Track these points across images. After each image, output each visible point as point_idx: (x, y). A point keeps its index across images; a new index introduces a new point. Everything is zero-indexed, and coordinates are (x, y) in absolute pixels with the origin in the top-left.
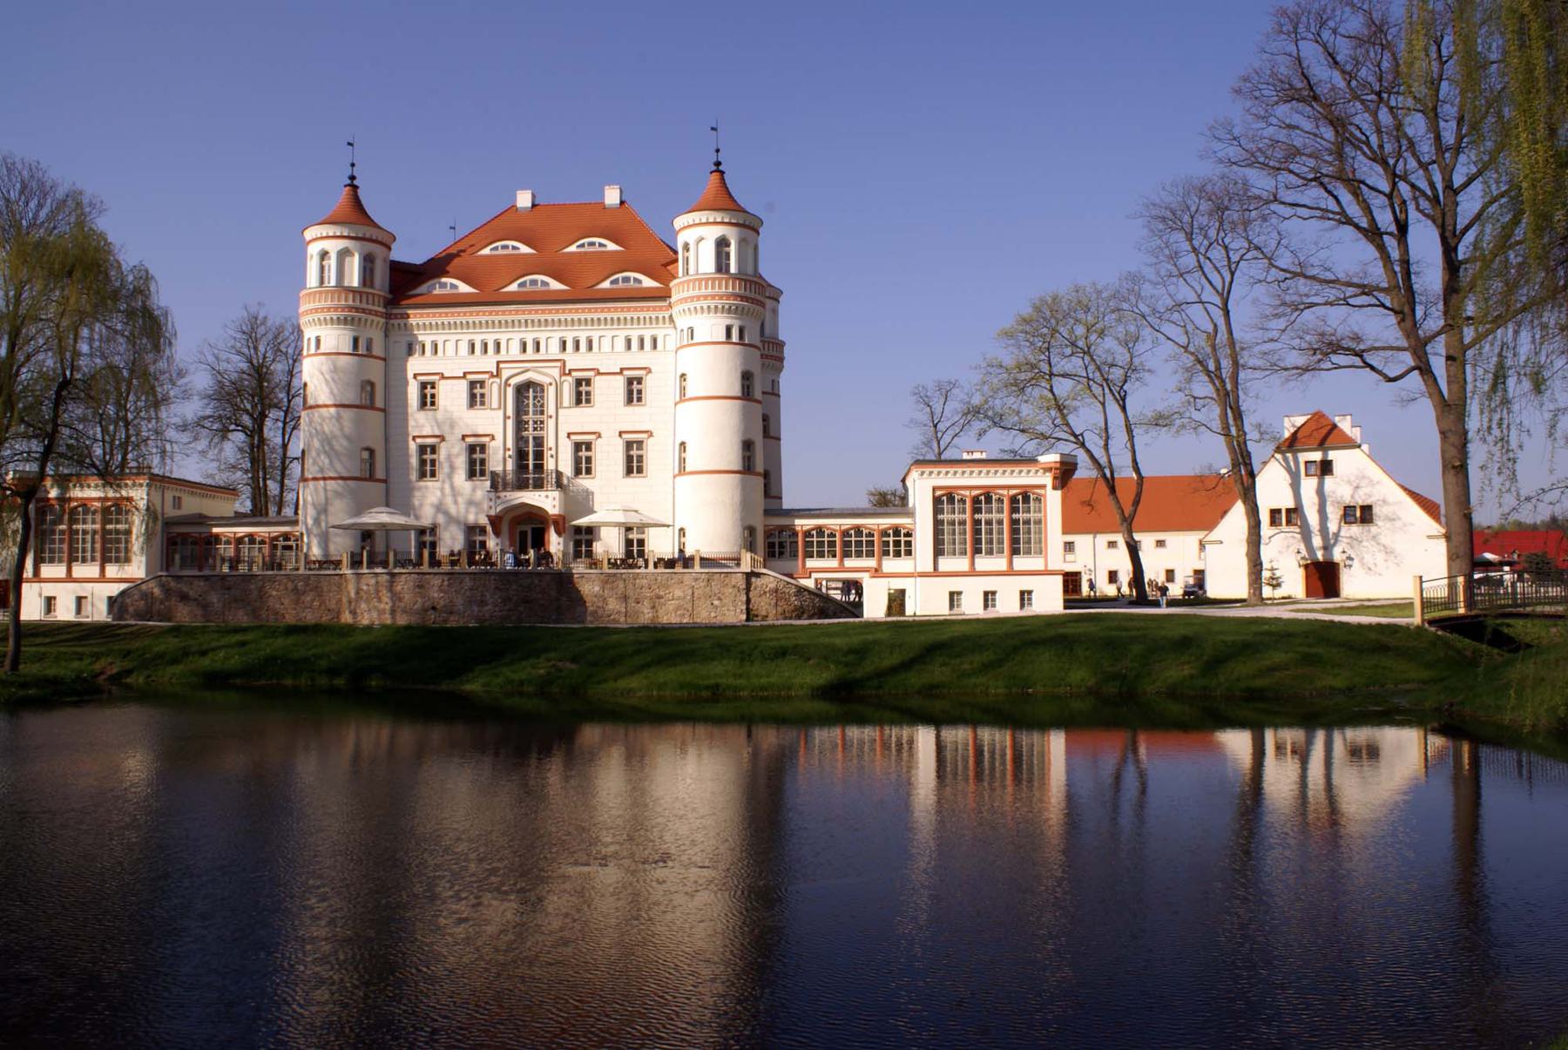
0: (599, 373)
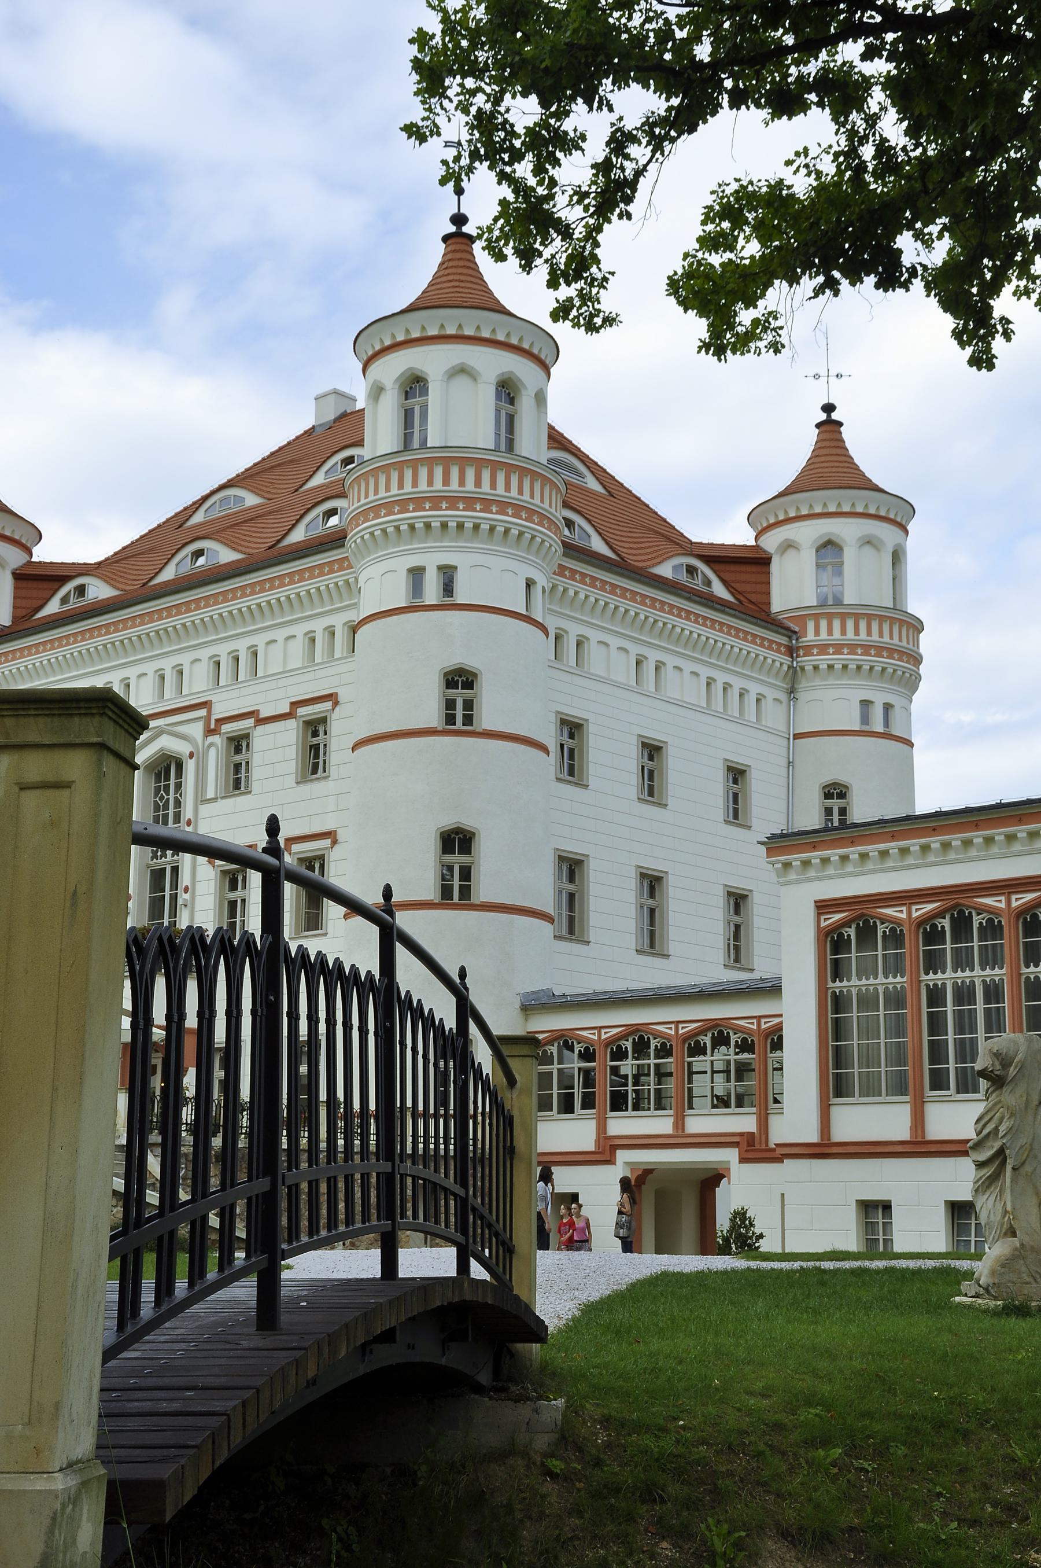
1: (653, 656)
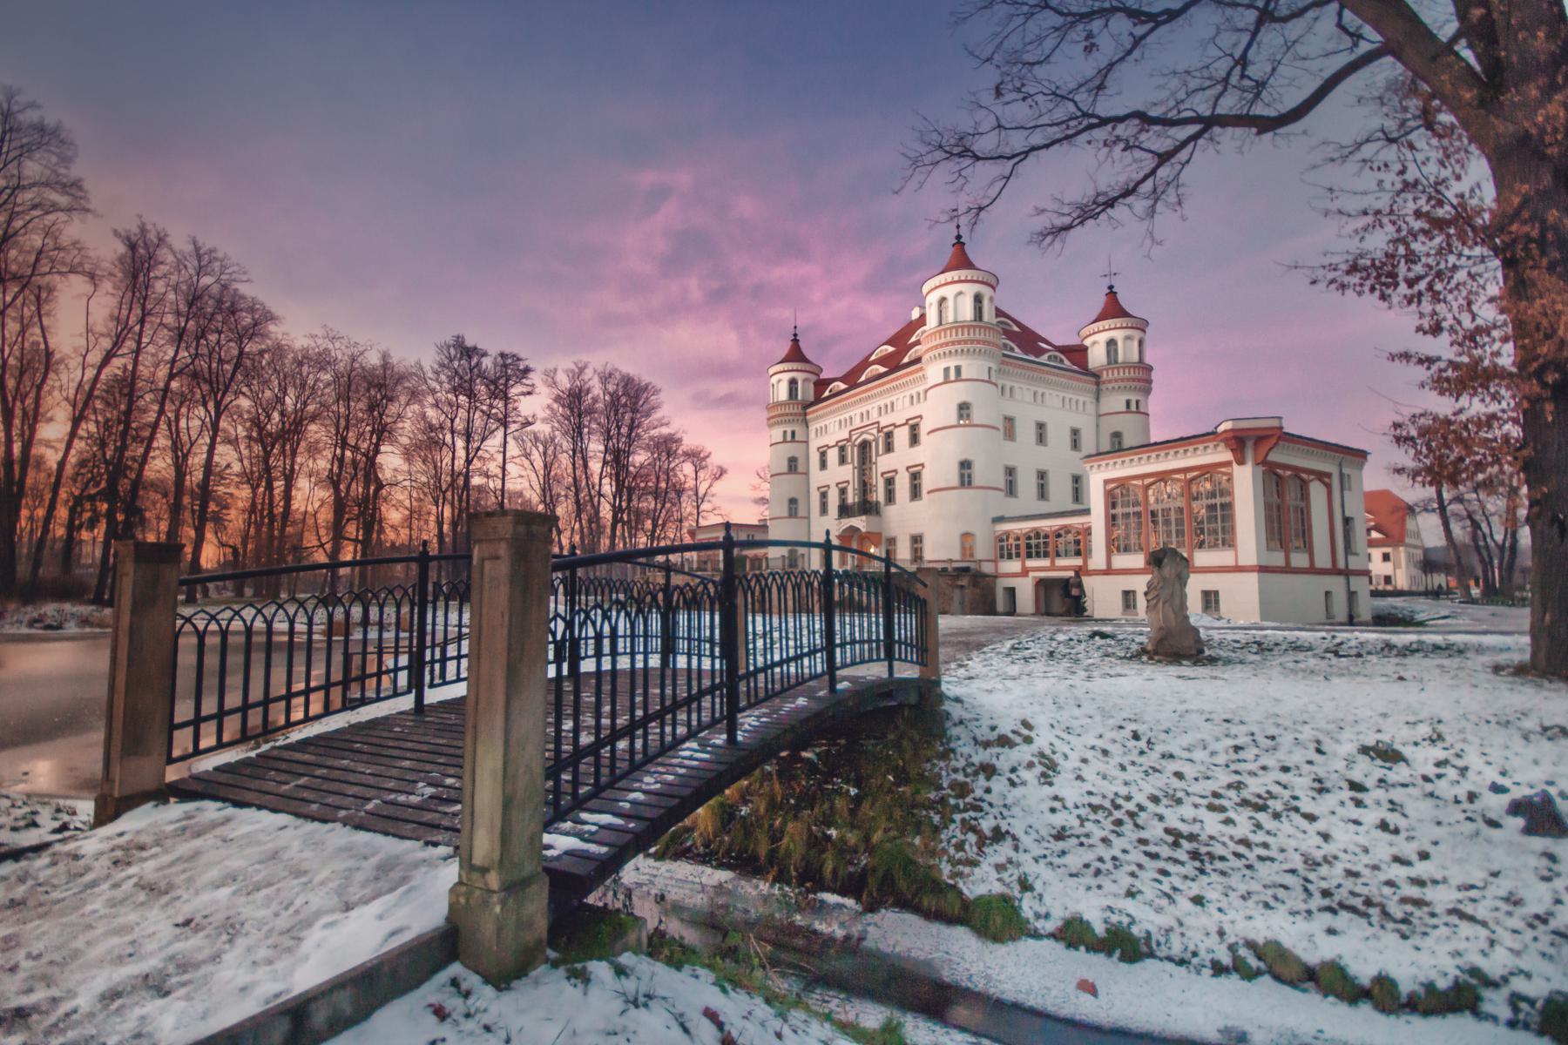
0: (896, 426)
1: (1040, 391)
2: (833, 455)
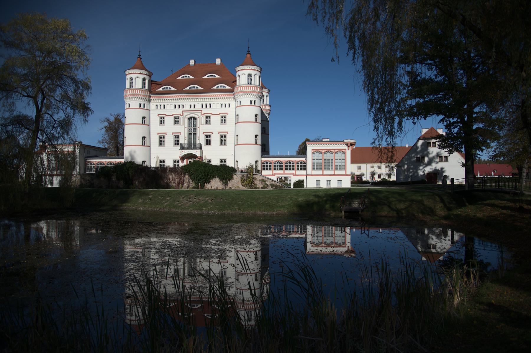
2: (170, 121)
